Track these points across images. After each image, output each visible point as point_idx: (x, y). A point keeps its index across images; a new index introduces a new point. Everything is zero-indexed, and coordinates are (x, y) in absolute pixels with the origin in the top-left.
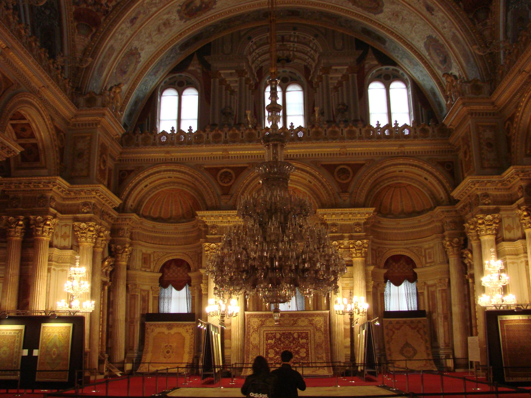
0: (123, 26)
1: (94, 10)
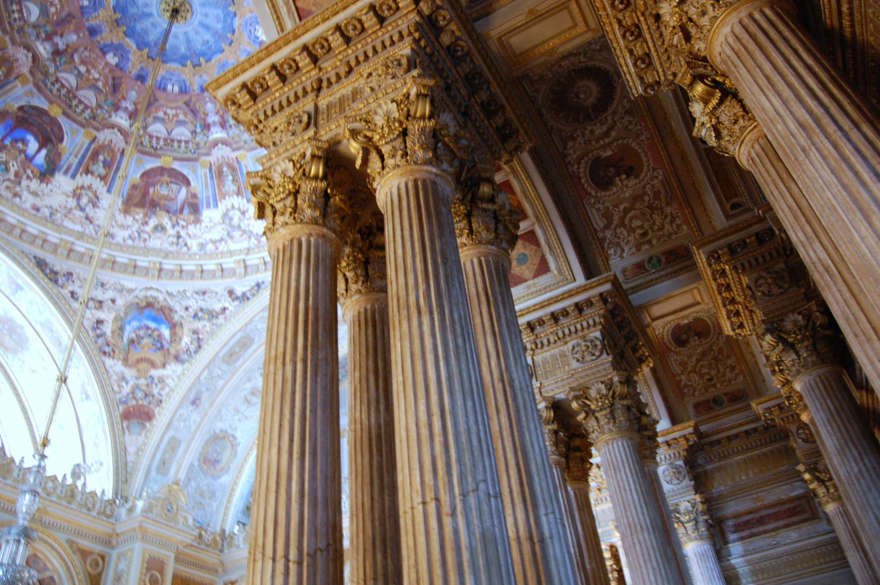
0: (181, 411)
1: (145, 403)
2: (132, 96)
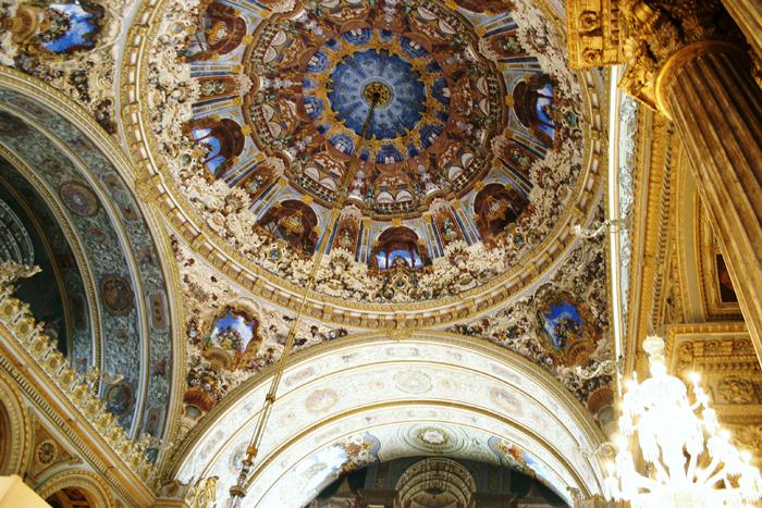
2: (450, 61)
